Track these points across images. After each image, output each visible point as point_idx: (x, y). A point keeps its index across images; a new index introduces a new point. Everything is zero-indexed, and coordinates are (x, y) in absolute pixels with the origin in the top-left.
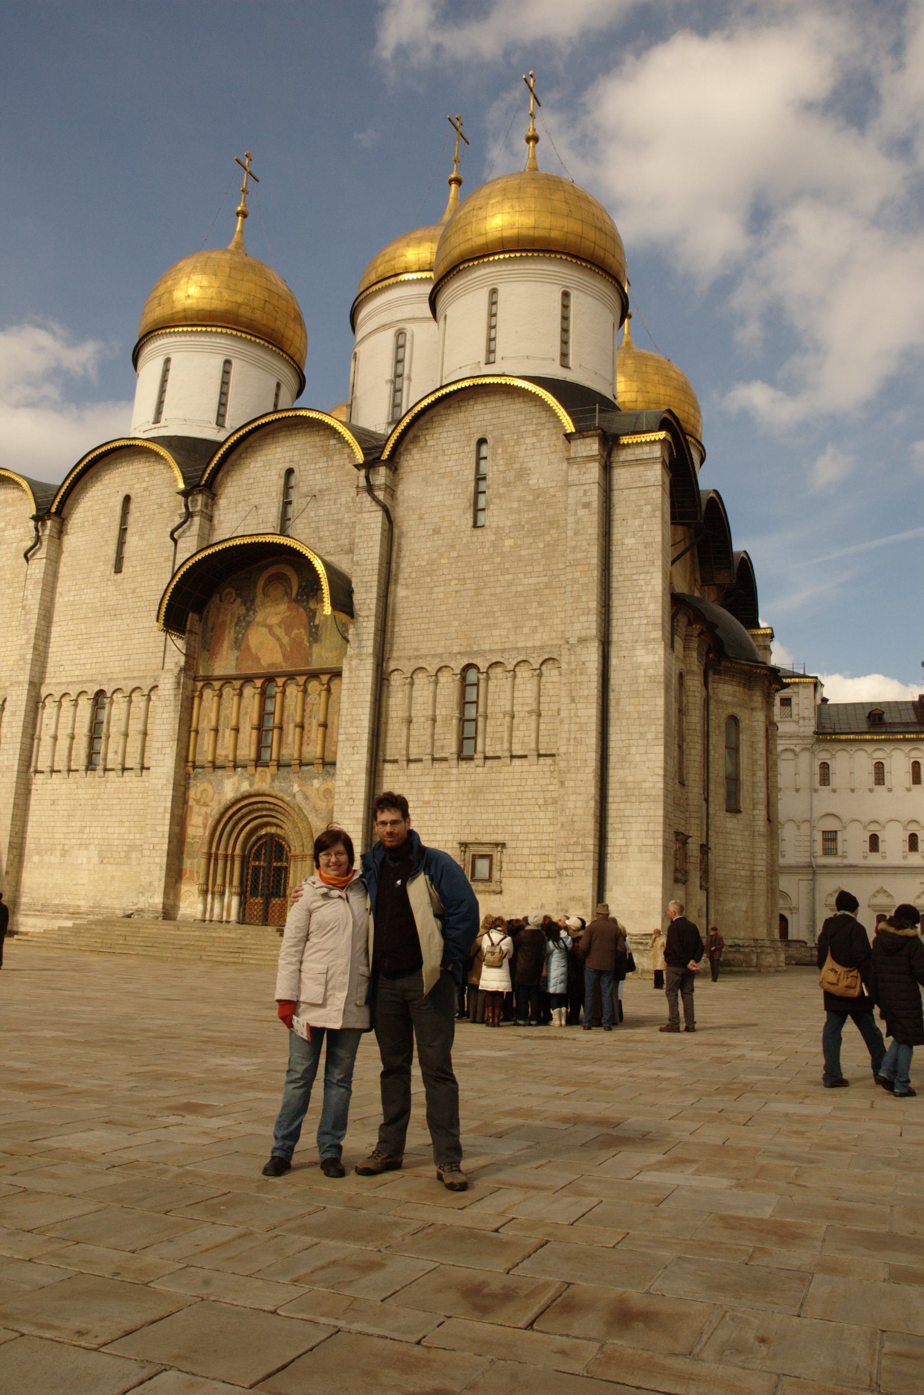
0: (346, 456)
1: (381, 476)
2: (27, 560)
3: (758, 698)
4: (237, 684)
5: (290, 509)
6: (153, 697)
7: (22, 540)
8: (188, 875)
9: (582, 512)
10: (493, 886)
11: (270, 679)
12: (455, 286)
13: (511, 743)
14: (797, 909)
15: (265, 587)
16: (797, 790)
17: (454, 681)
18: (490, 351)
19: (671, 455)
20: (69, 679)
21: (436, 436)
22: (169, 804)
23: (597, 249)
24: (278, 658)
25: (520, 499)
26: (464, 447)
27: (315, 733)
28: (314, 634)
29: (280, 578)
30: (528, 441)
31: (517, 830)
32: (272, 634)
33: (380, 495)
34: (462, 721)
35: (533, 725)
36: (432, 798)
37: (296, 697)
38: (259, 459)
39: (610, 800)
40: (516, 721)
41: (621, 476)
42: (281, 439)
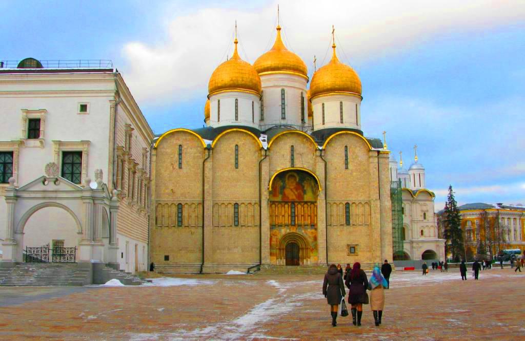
4: (283, 204)
7: (195, 153)
9: (374, 169)
10: (356, 254)
11: (293, 203)
18: (342, 119)
22: (269, 236)
24: (294, 197)
25: (357, 163)
28: (305, 192)
32: (292, 191)
41: (381, 160)
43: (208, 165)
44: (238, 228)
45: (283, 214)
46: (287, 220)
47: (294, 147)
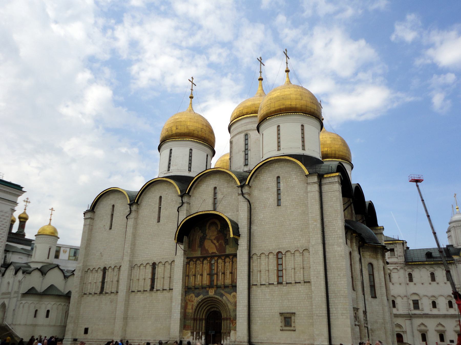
0: (234, 183)
1: (246, 190)
2: (127, 219)
3: (379, 256)
4: (201, 260)
5: (216, 200)
6: (172, 265)
8: (187, 327)
11: (212, 257)
12: (266, 124)
13: (295, 278)
14: (406, 331)
15: (209, 226)
16: (400, 284)
17: (274, 257)
18: (279, 146)
19: (341, 179)
20: (143, 259)
21: (263, 176)
22: (180, 302)
23: (312, 109)
24: (215, 250)
26: (272, 179)
27: (228, 276)
29: (214, 224)
30: (293, 177)
31: (299, 308)
32: (212, 242)
33: (246, 196)
34: (278, 271)
35: (302, 271)
36: (269, 297)
37: (222, 263)
38: (205, 184)
39: (330, 297)
40: (296, 270)
41: (325, 188)
42: (212, 177)
43: (131, 222)
44: (153, 294)
45: (201, 273)
46: (206, 281)
47: (218, 188)
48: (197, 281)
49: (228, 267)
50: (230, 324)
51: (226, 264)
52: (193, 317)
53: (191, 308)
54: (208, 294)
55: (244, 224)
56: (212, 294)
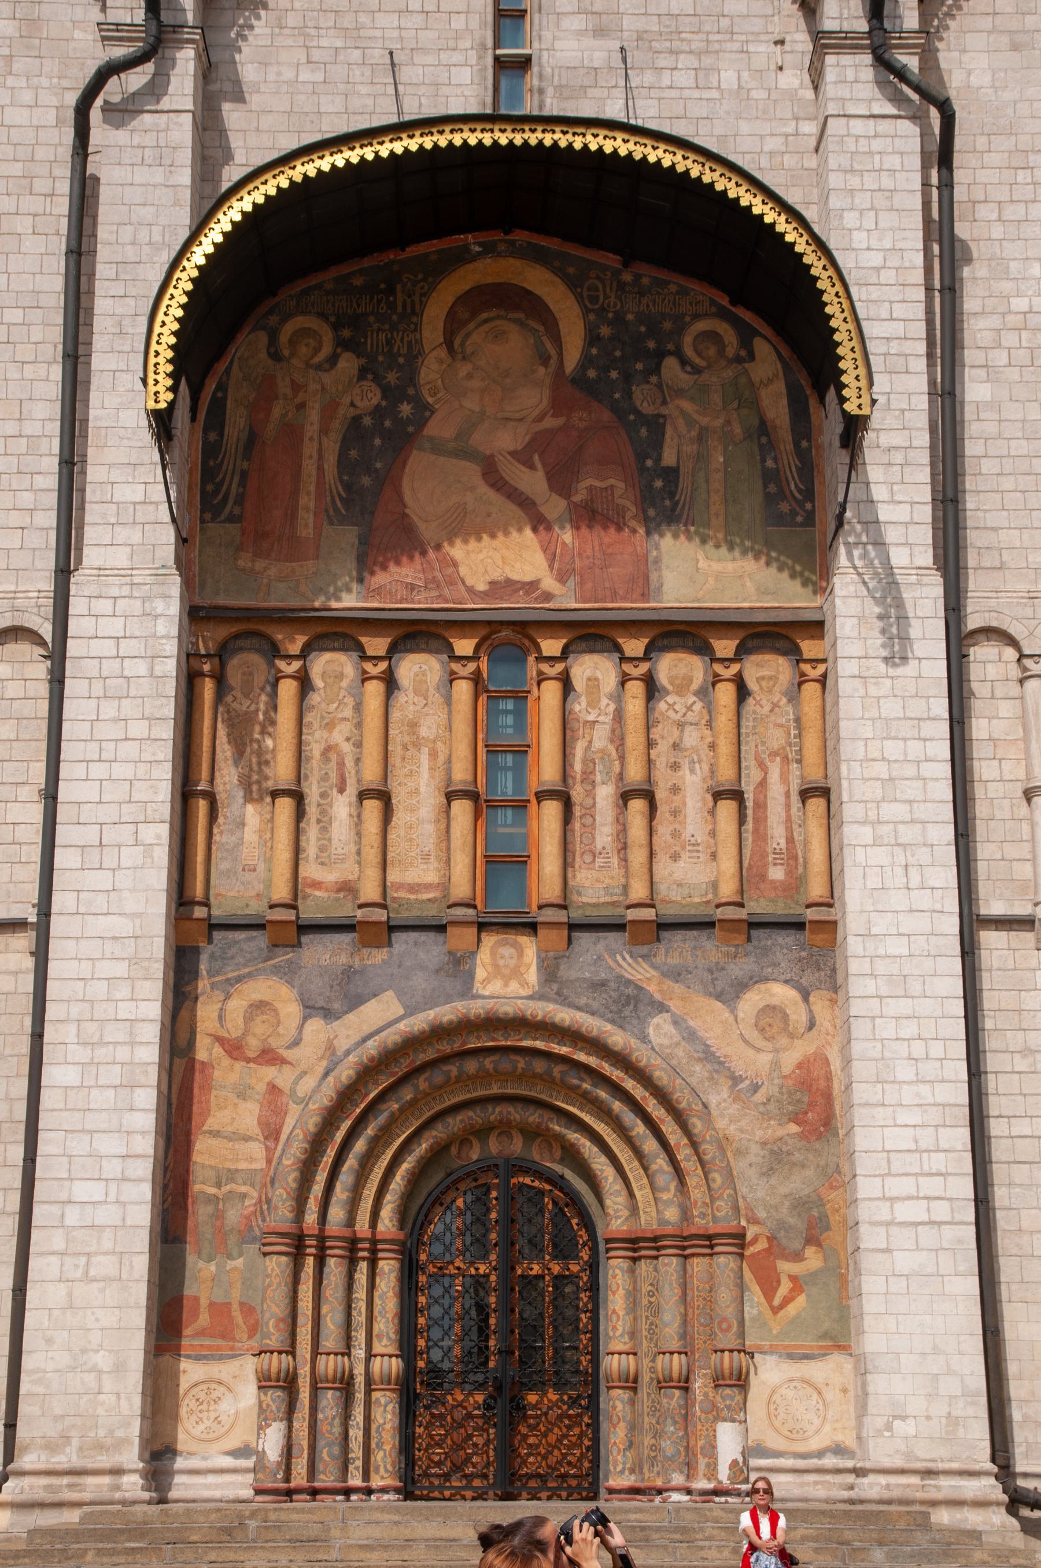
8: (204, 1319)
15: (453, 326)
48: (322, 849)
49: (691, 738)
50: (741, 1286)
51: (662, 706)
52: (282, 1215)
53: (263, 1123)
54: (467, 991)
55: (896, 329)
56: (514, 988)
